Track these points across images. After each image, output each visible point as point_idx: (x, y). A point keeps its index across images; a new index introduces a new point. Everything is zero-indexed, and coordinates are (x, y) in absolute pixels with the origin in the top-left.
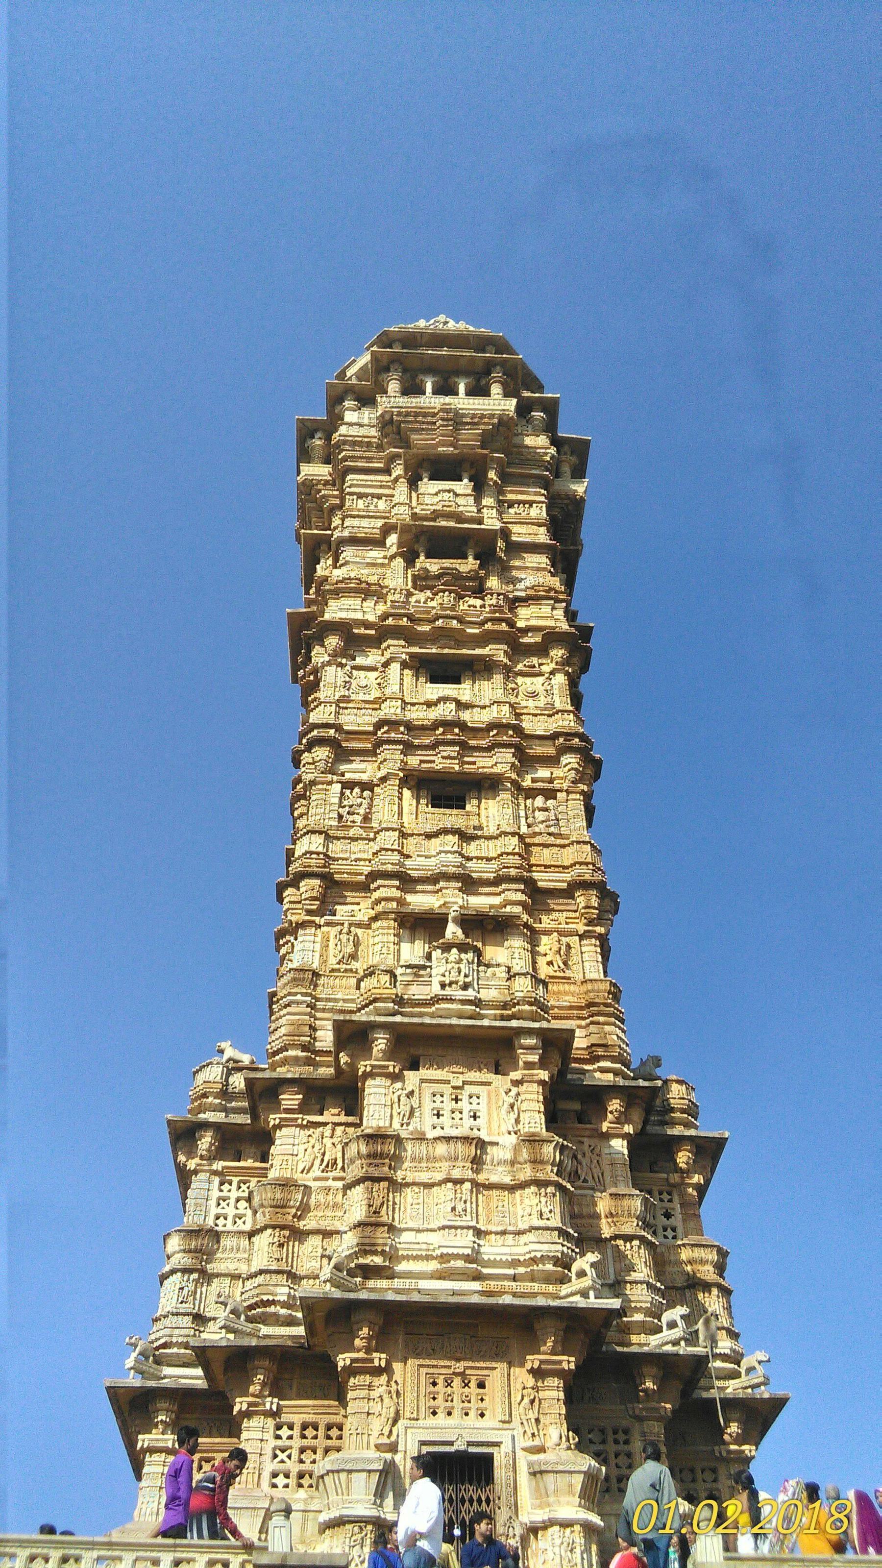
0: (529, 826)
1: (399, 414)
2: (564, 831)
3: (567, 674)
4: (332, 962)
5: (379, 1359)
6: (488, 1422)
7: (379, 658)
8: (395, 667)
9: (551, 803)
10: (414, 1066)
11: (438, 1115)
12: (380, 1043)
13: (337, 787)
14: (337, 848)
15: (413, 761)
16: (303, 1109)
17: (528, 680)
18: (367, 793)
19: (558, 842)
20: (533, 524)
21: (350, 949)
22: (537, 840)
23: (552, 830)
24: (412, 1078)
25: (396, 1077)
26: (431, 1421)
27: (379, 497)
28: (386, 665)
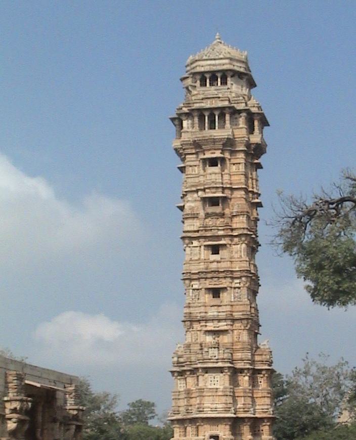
0: (234, 298)
1: (198, 140)
2: (241, 300)
3: (245, 244)
4: (194, 340)
5: (202, 424)
6: (218, 431)
7: (198, 243)
8: (202, 247)
9: (239, 290)
10: (207, 373)
11: (211, 381)
12: (200, 371)
13: (191, 291)
14: (192, 310)
15: (208, 281)
16: (190, 374)
17: (236, 246)
18: (198, 291)
19: (241, 303)
20: (240, 174)
21: (196, 338)
22: (235, 303)
23: (239, 300)
24: (207, 375)
25: (203, 376)
26: (210, 432)
27: (196, 166)
28: (200, 247)
